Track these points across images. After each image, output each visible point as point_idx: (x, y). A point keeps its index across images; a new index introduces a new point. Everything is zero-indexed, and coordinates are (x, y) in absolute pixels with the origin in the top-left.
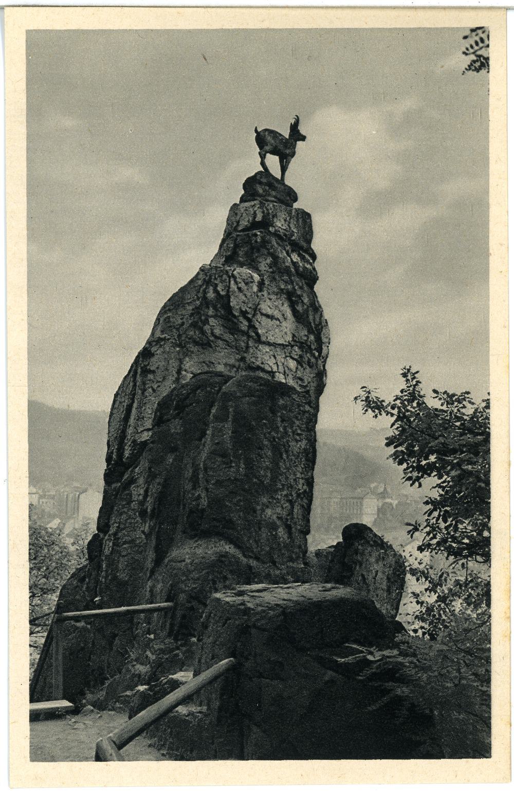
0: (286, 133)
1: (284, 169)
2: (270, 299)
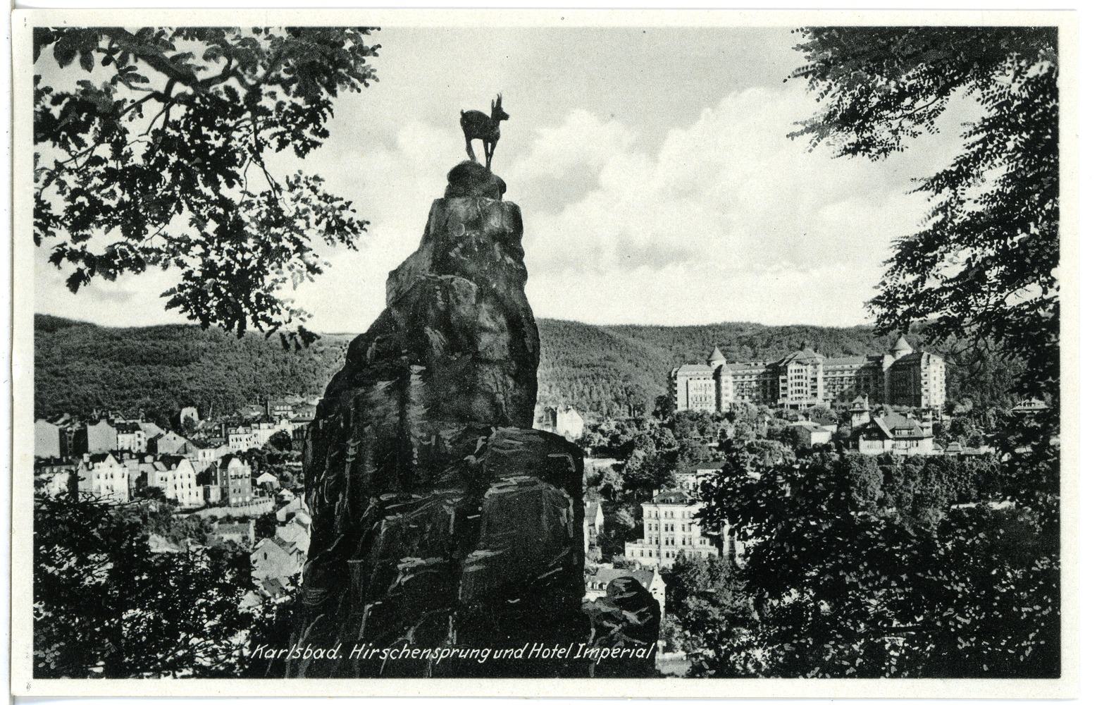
0: (489, 113)
1: (489, 155)
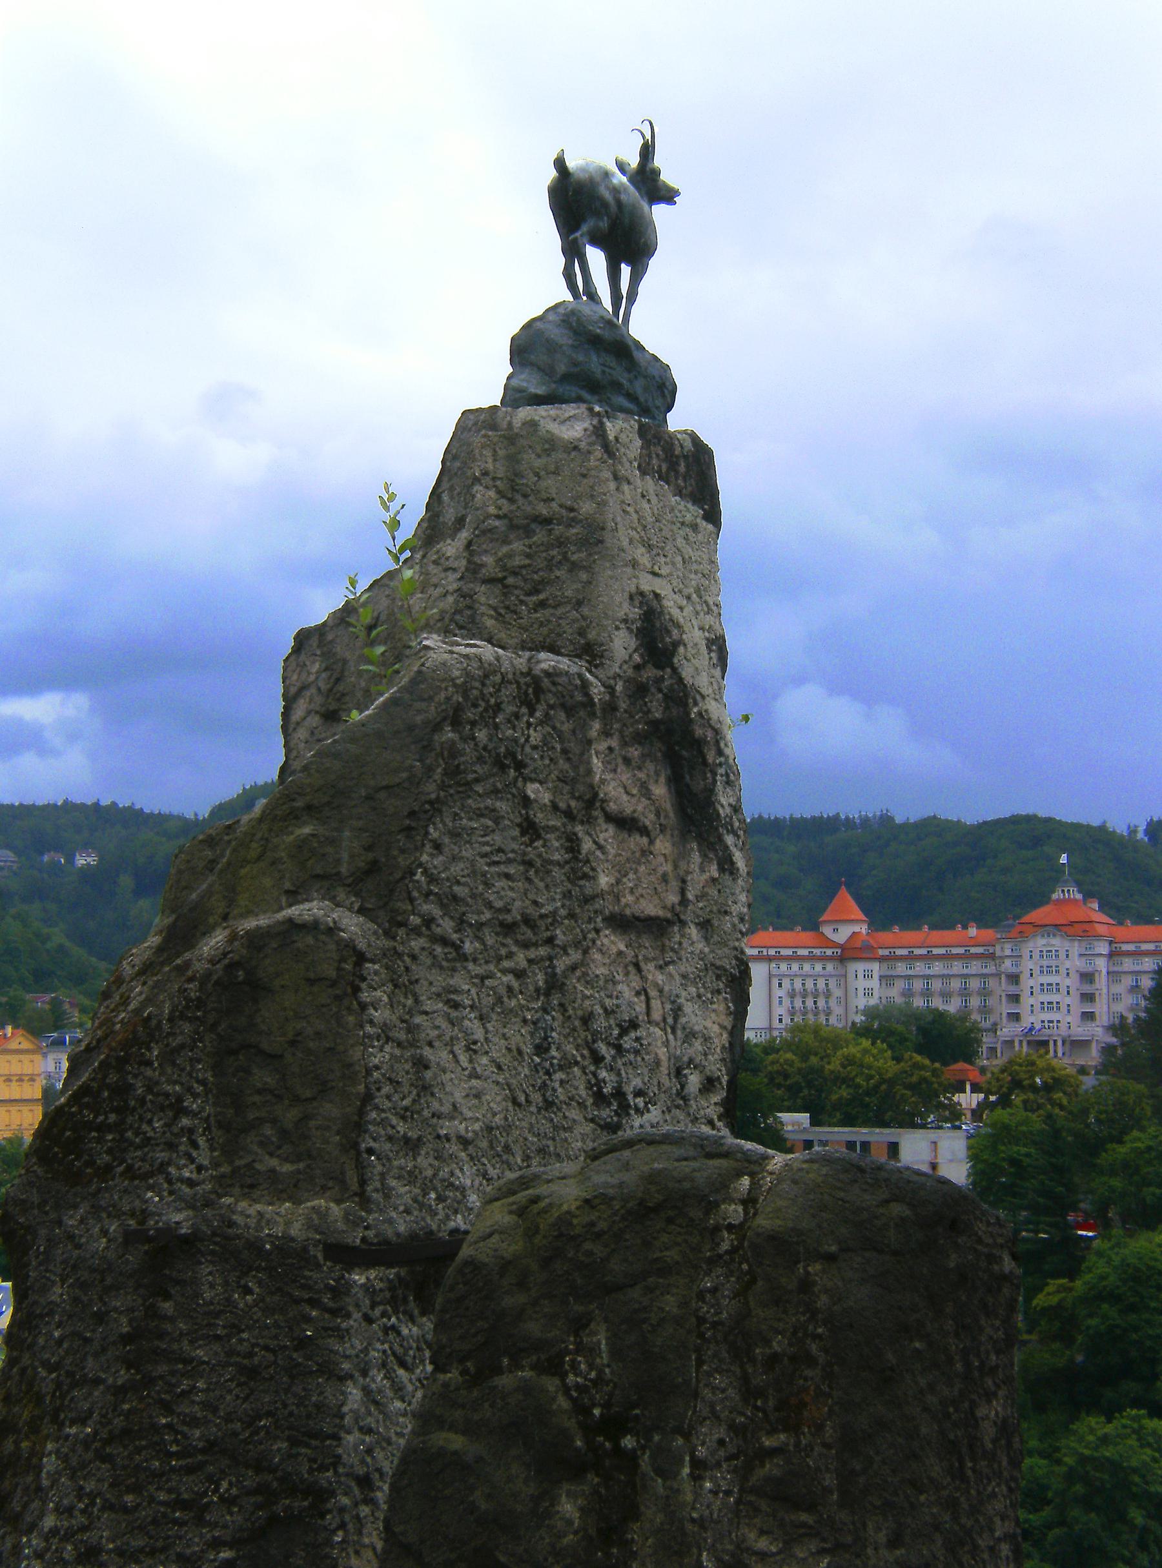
2: (627, 761)
